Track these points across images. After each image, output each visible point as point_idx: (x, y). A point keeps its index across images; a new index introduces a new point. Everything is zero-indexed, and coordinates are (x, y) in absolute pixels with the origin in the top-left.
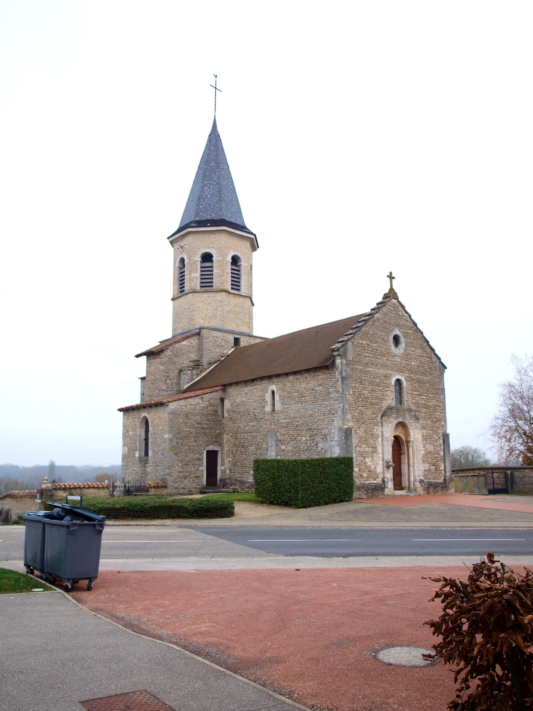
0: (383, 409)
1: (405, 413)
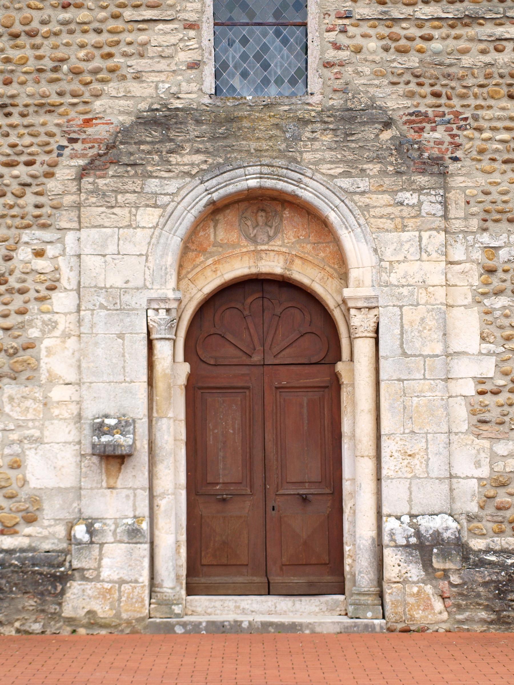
1: (297, 138)
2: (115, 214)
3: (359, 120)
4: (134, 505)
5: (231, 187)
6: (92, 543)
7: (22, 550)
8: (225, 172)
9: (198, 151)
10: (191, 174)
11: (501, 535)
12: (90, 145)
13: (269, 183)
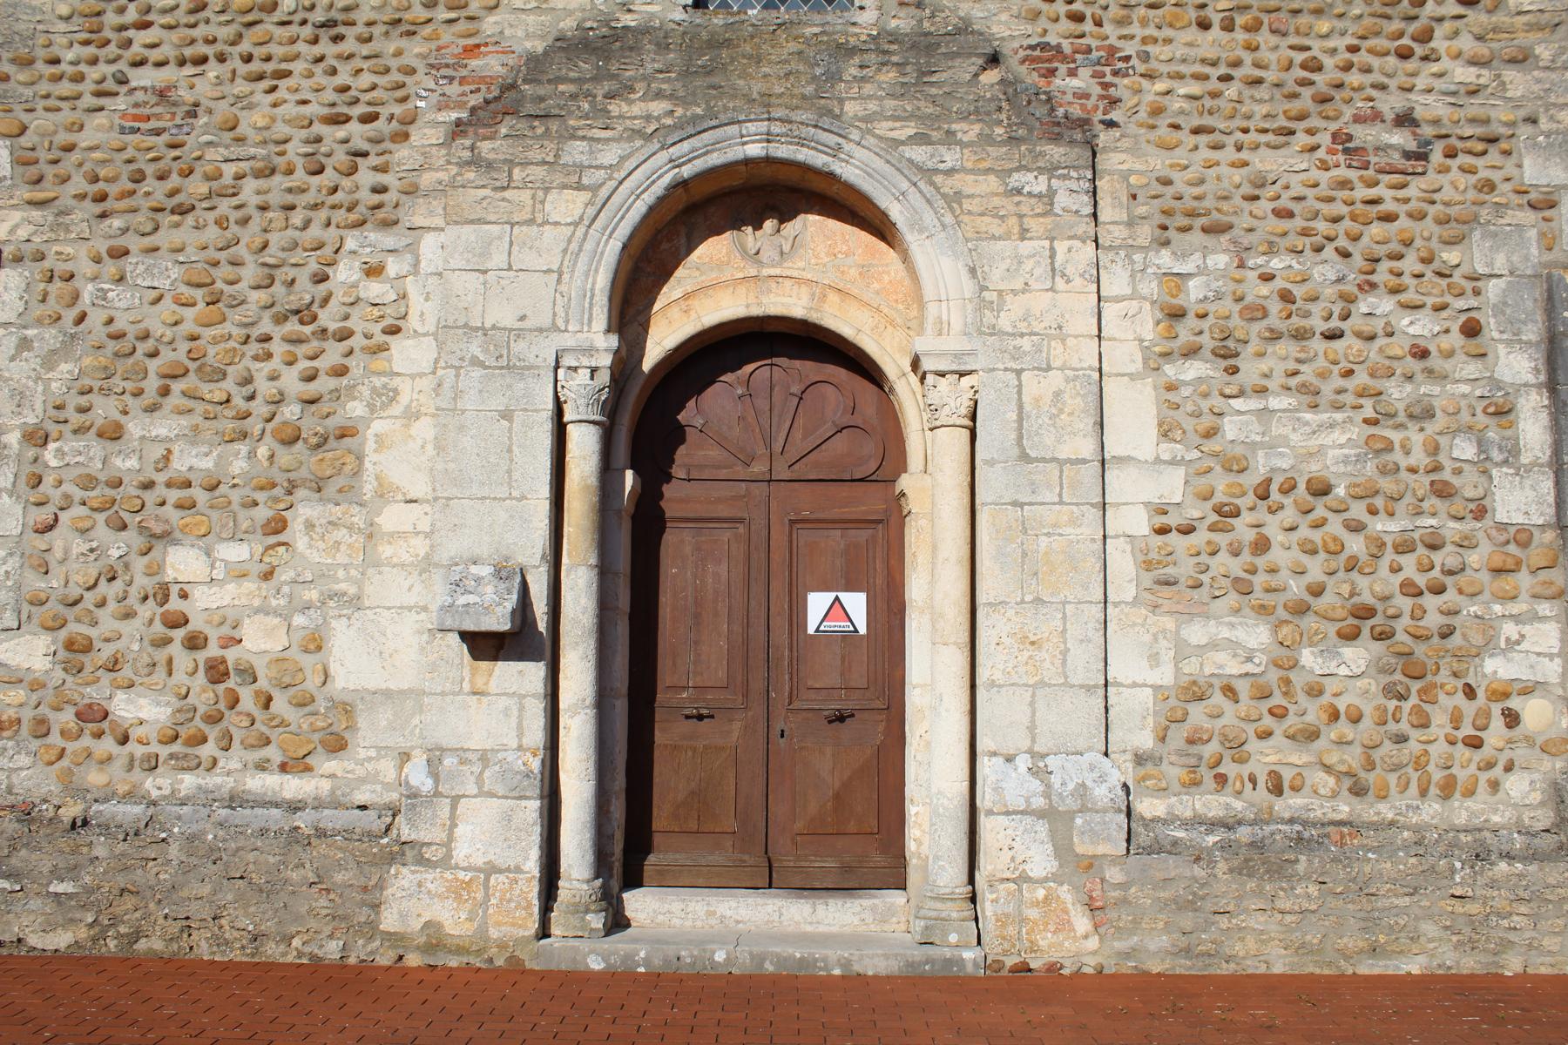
0: (491, 65)
1: (834, 77)
2: (508, 201)
3: (943, 50)
4: (520, 727)
5: (715, 155)
6: (437, 794)
7: (319, 805)
8: (704, 131)
9: (659, 95)
10: (646, 133)
11: (1193, 789)
12: (473, 87)
13: (782, 151)
